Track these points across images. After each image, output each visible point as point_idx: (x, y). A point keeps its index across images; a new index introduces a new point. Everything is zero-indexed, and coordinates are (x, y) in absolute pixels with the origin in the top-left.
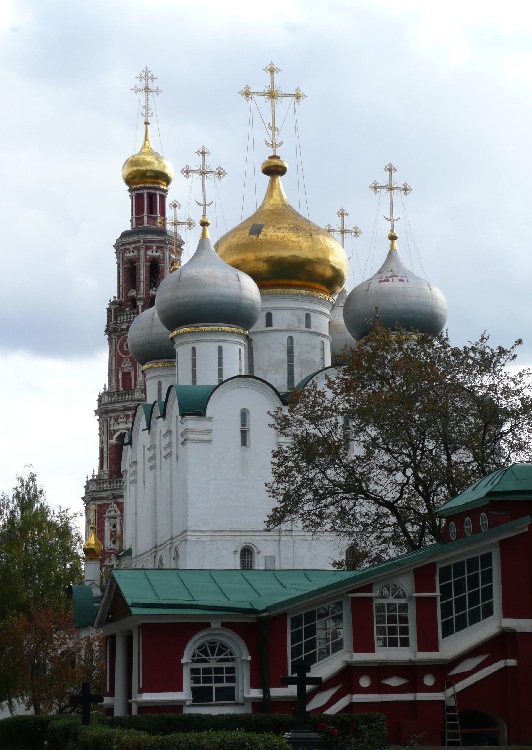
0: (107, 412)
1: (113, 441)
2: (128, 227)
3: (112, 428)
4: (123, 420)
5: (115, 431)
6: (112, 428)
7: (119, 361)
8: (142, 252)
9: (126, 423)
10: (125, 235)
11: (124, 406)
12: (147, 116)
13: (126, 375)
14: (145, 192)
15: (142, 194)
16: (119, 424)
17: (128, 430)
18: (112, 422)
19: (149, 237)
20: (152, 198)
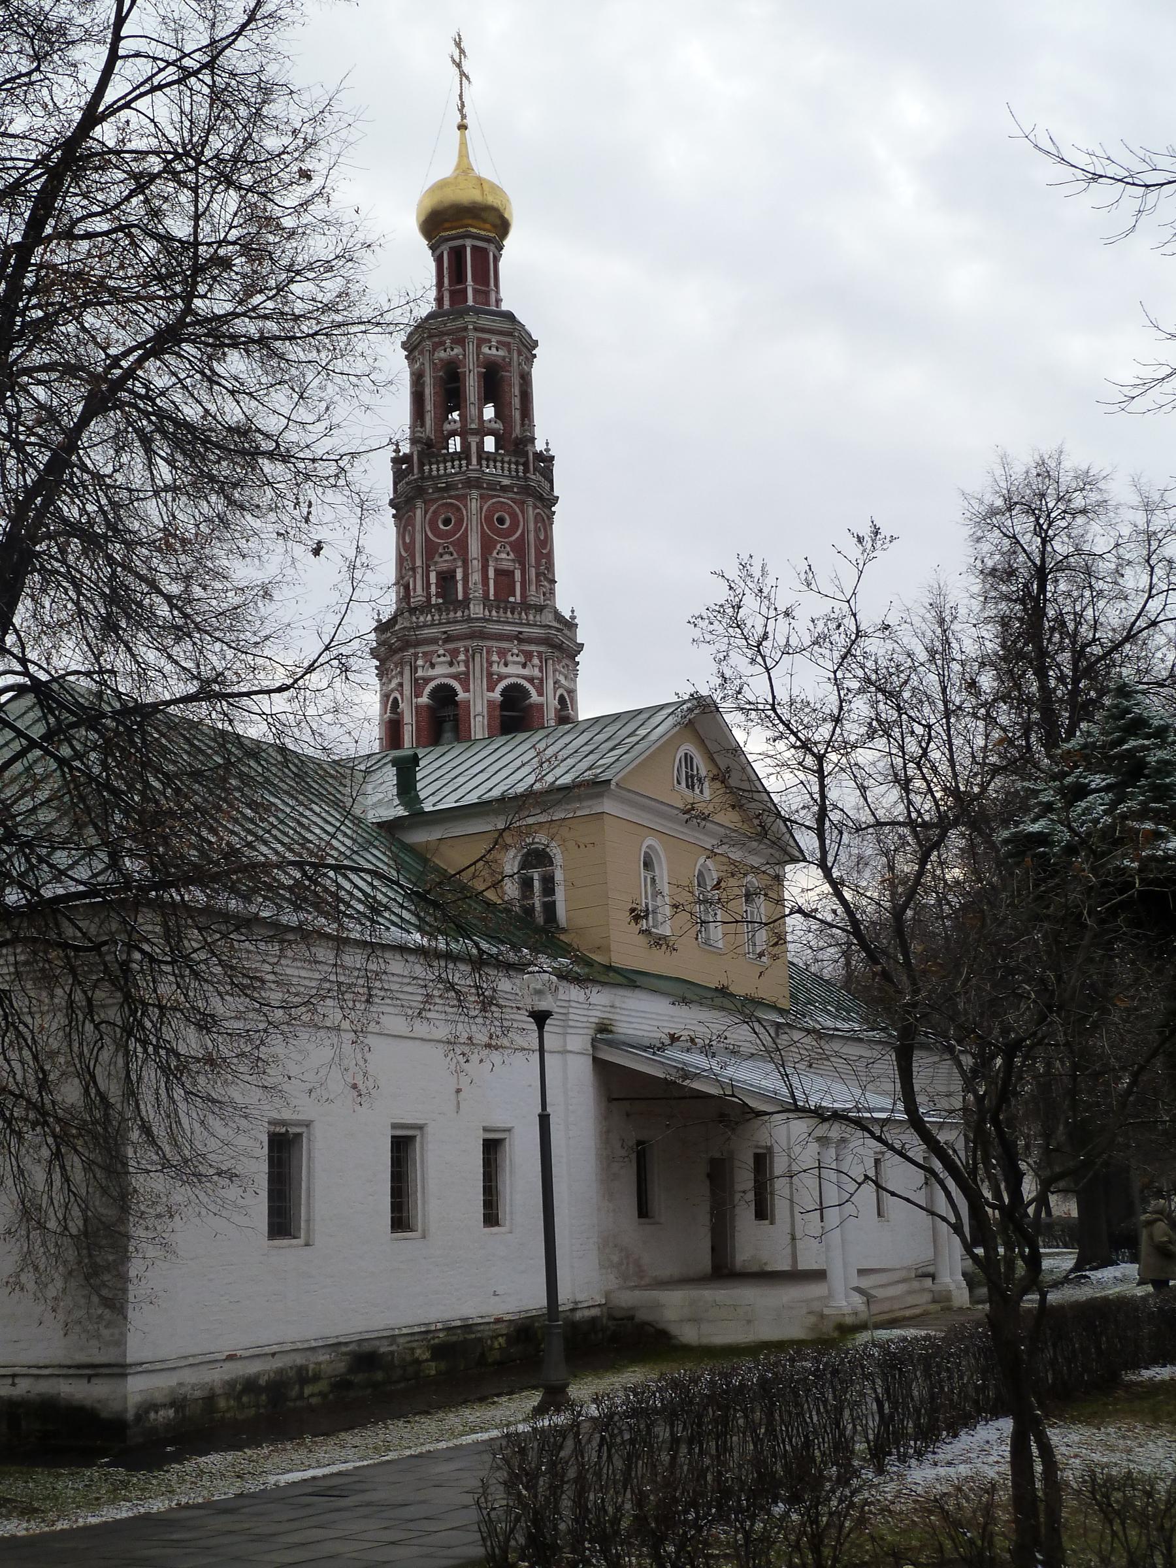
0: (406, 644)
1: (424, 700)
3: (420, 673)
4: (442, 659)
5: (427, 680)
6: (420, 673)
7: (431, 551)
8: (471, 348)
9: (451, 664)
10: (431, 316)
11: (445, 632)
14: (469, 243)
15: (464, 247)
16: (433, 666)
17: (455, 677)
18: (420, 662)
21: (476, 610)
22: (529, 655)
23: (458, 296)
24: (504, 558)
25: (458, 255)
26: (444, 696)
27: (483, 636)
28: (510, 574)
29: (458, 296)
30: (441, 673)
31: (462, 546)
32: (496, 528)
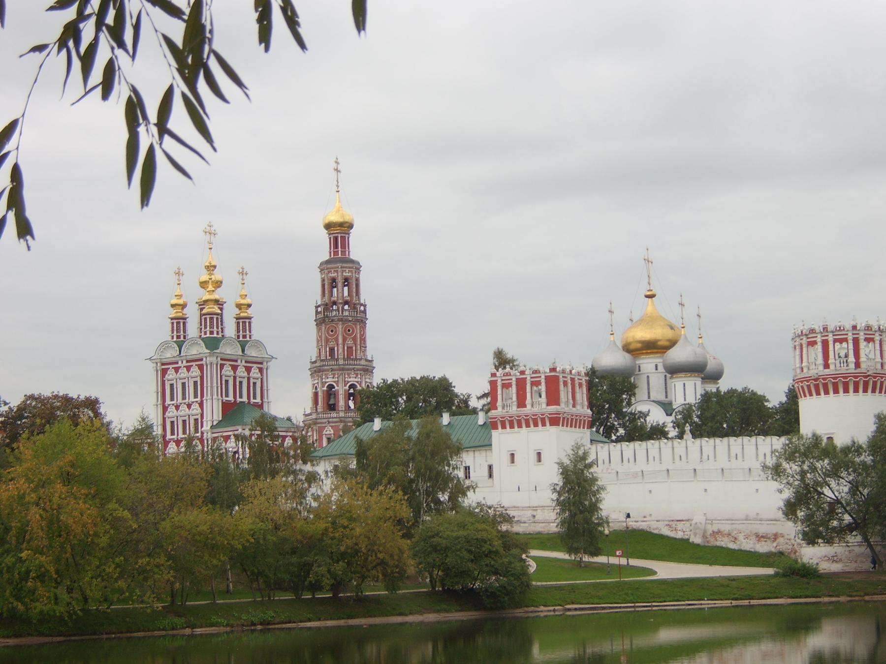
0: (320, 371)
1: (325, 388)
2: (326, 257)
7: (327, 340)
10: (327, 262)
12: (338, 186)
13: (332, 350)
19: (344, 265)
21: (341, 362)
22: (357, 375)
23: (336, 253)
24: (350, 342)
25: (336, 239)
26: (331, 387)
27: (343, 369)
28: (352, 348)
29: (336, 253)
30: (330, 381)
31: (337, 340)
32: (347, 331)
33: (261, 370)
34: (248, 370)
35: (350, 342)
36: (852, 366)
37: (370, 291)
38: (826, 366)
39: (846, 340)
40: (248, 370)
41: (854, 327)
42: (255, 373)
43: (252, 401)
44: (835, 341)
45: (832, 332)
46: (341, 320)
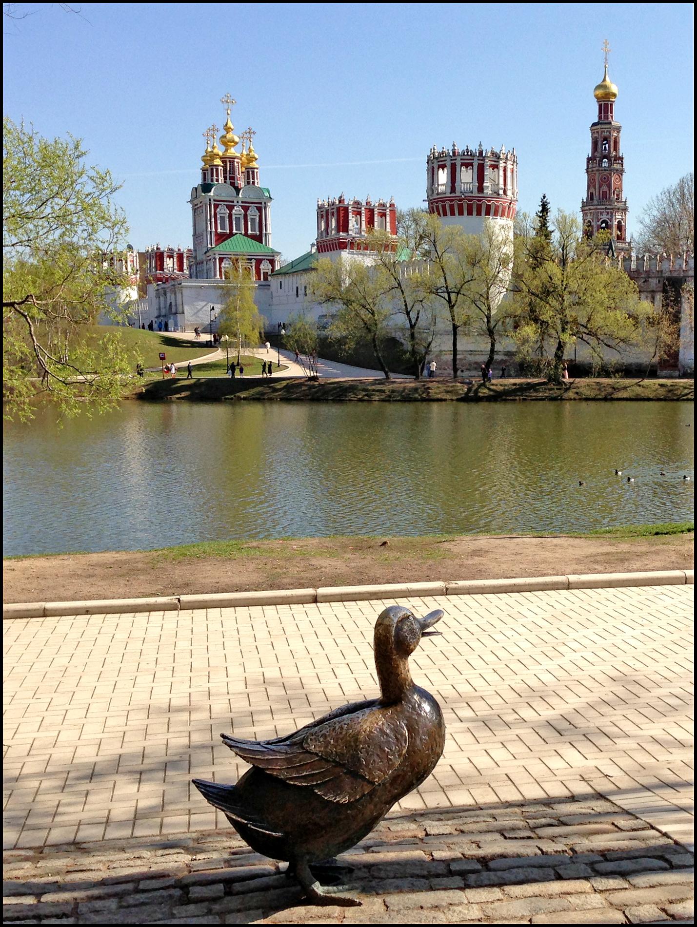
2: (596, 120)
10: (594, 125)
13: (592, 194)
20: (606, 105)
24: (605, 188)
29: (600, 118)
33: (259, 209)
34: (246, 209)
35: (605, 188)
36: (476, 190)
37: (627, 146)
38: (453, 190)
39: (472, 165)
40: (246, 209)
41: (481, 153)
42: (253, 212)
43: (250, 232)
44: (462, 165)
45: (437, 158)
46: (598, 170)
